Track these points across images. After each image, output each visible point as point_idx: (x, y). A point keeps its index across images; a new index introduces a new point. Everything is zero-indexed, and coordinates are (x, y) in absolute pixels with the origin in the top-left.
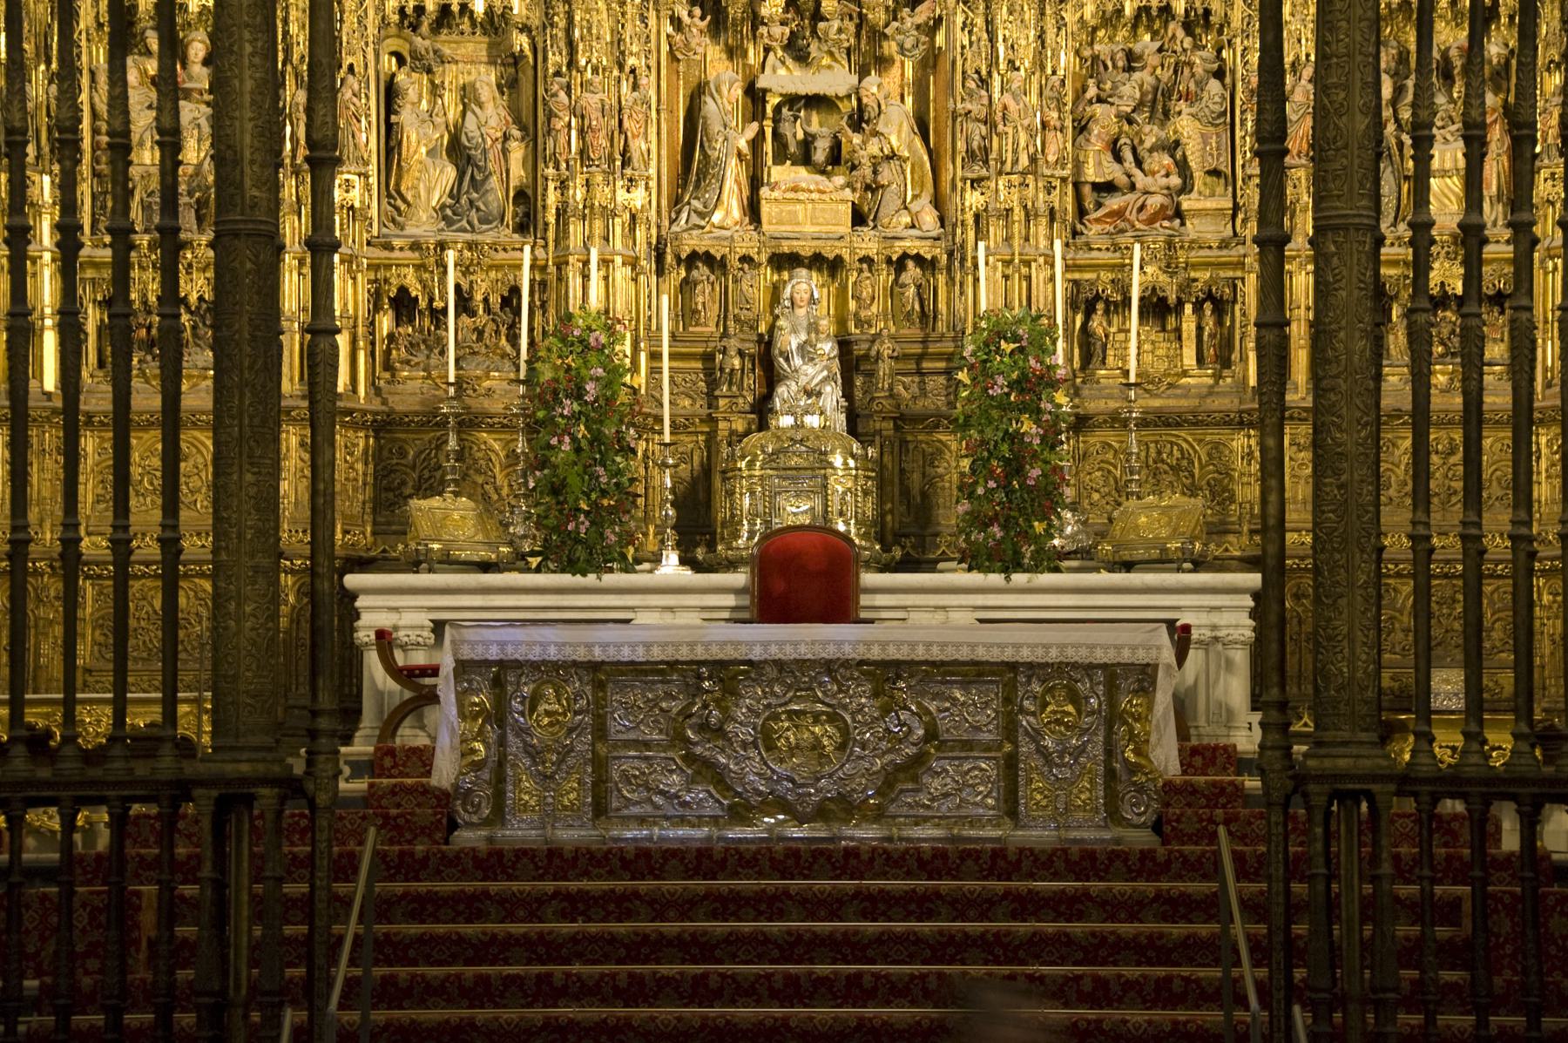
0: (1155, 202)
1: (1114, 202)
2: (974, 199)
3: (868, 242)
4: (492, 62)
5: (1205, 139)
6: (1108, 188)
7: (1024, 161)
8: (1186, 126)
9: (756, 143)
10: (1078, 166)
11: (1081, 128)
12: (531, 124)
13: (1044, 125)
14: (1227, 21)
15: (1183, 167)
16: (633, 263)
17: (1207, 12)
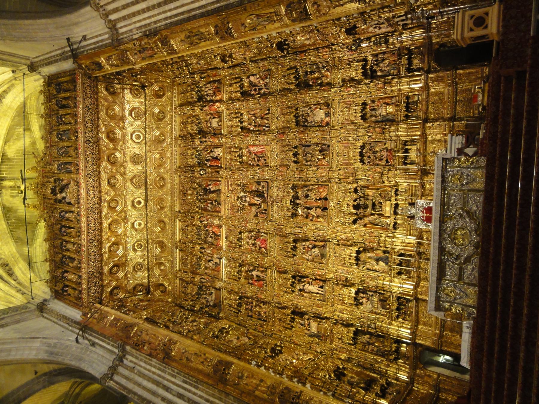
0: (389, 154)
1: (389, 160)
2: (386, 182)
3: (393, 199)
4: (365, 253)
5: (380, 146)
6: (387, 161)
7: (379, 174)
8: (377, 149)
9: (378, 214)
10: (383, 166)
11: (377, 165)
12: (373, 250)
13: (375, 171)
14: (363, 143)
15: (384, 149)
16: (394, 237)
17: (361, 146)
